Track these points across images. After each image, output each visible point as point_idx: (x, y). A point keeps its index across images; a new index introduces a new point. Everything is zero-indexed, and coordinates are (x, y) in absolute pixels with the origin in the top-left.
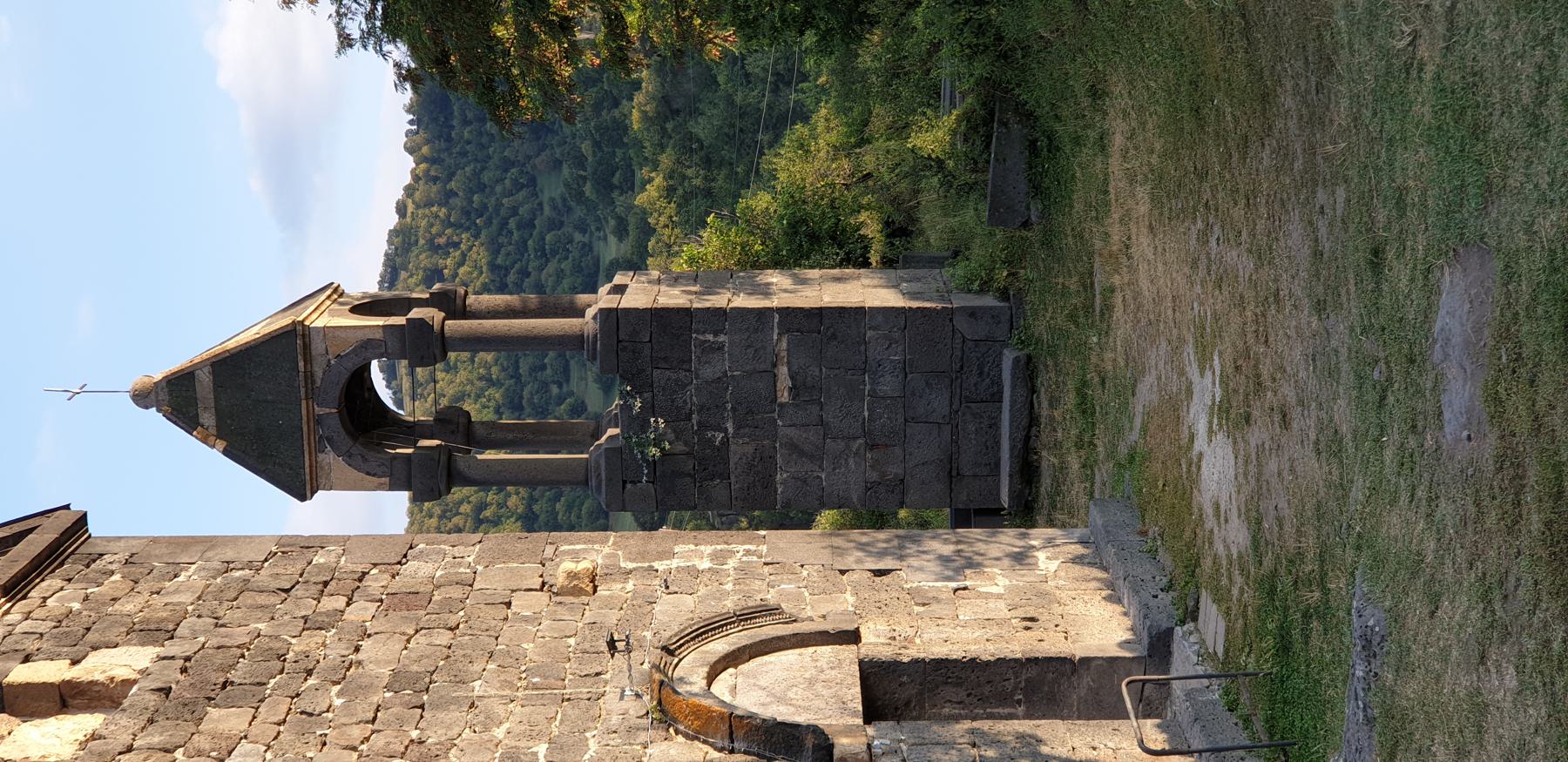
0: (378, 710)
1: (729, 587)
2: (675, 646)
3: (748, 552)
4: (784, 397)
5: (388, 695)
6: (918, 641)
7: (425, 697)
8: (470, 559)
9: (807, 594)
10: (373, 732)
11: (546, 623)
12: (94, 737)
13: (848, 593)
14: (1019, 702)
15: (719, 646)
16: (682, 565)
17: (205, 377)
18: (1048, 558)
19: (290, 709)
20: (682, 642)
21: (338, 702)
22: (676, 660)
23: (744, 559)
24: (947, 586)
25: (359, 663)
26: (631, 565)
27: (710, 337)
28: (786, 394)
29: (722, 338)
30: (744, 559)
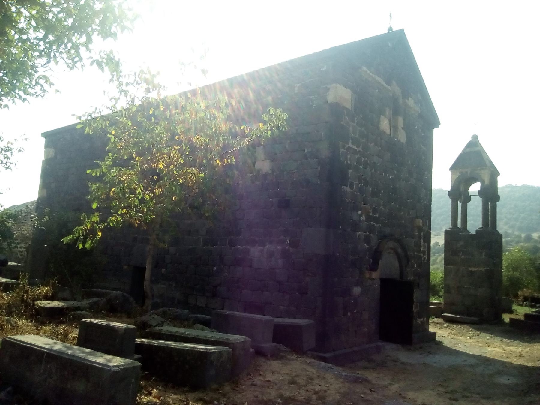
1: (416, 253)
3: (425, 258)
4: (470, 269)
5: (392, 186)
8: (425, 202)
9: (413, 269)
12: (385, 133)
15: (400, 251)
16: (422, 244)
17: (477, 149)
18: (421, 321)
23: (423, 258)
26: (422, 234)
27: (484, 254)
28: (471, 269)
29: (484, 256)
30: (423, 258)
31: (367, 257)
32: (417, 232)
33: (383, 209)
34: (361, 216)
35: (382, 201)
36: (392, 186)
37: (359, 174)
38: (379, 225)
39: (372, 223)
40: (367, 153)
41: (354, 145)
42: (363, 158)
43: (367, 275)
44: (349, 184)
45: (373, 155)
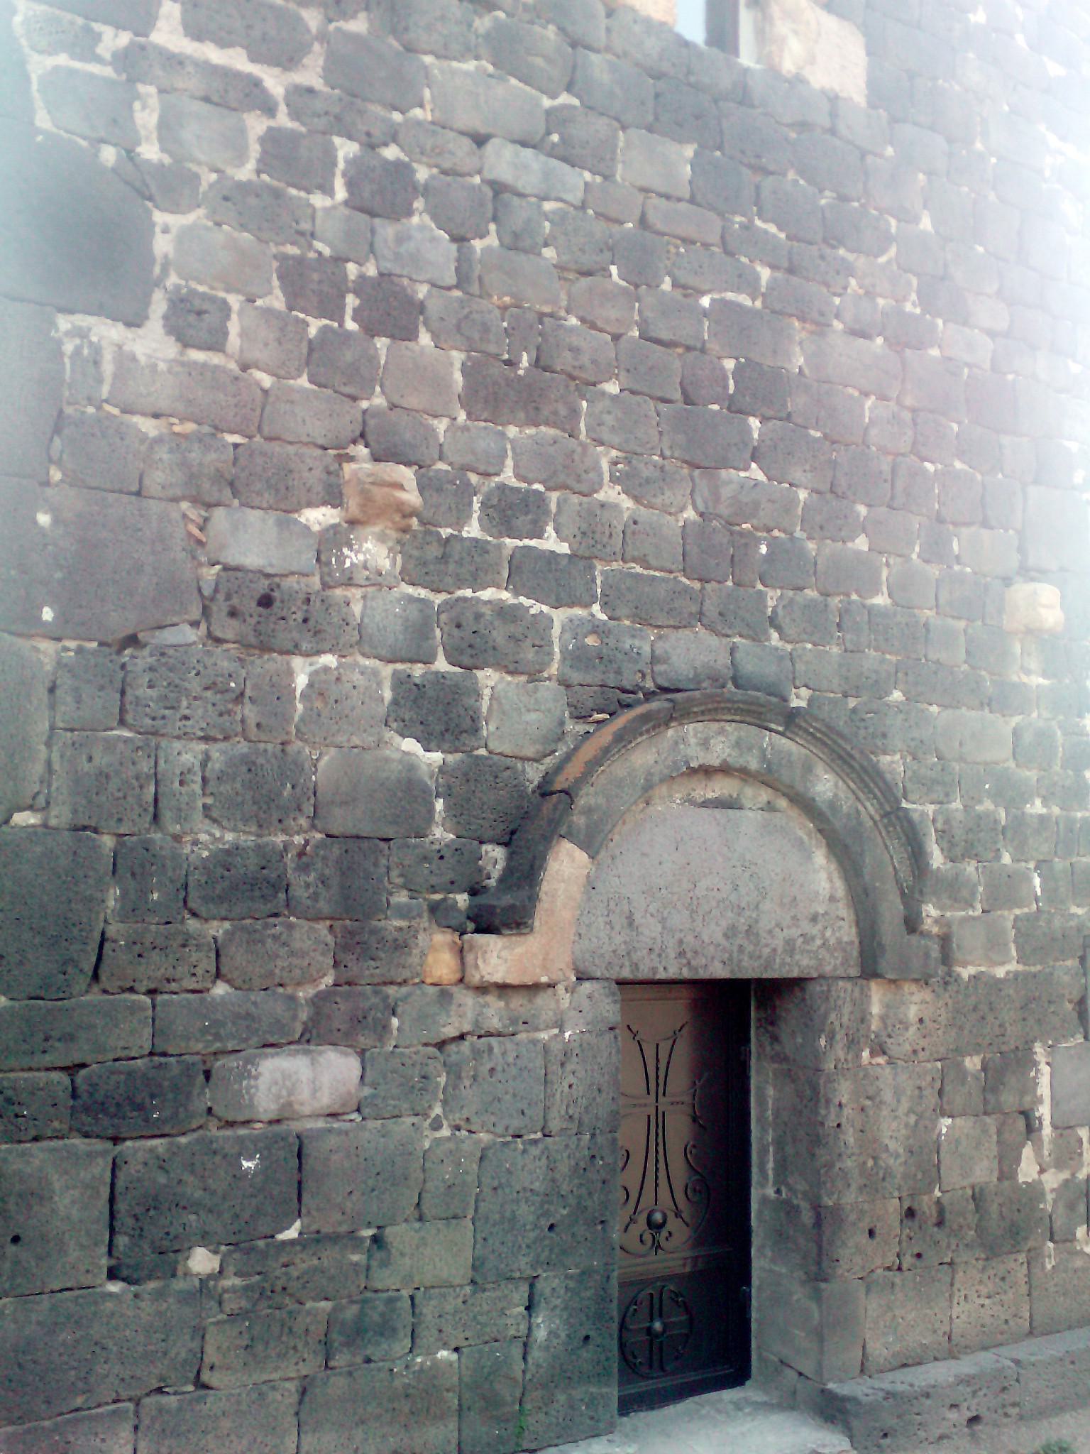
0: (689, 349)
2: (804, 725)
6: (881, 1060)
7: (715, 407)
9: (1017, 912)
10: (616, 338)
11: (934, 571)
13: (1020, 968)
14: (778, 1192)
19: (693, 242)
20: (818, 735)
21: (705, 301)
22: (781, 729)
24: (1040, 1100)
25: (822, 334)
31: (441, 834)
32: (1033, 664)
33: (627, 503)
34: (333, 539)
35: (605, 458)
36: (729, 364)
37: (292, 250)
38: (579, 612)
39: (487, 594)
40: (397, 117)
41: (222, 44)
42: (337, 140)
43: (442, 965)
44: (159, 305)
45: (480, 140)
